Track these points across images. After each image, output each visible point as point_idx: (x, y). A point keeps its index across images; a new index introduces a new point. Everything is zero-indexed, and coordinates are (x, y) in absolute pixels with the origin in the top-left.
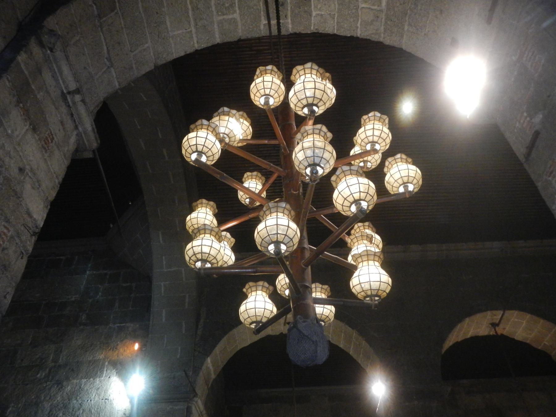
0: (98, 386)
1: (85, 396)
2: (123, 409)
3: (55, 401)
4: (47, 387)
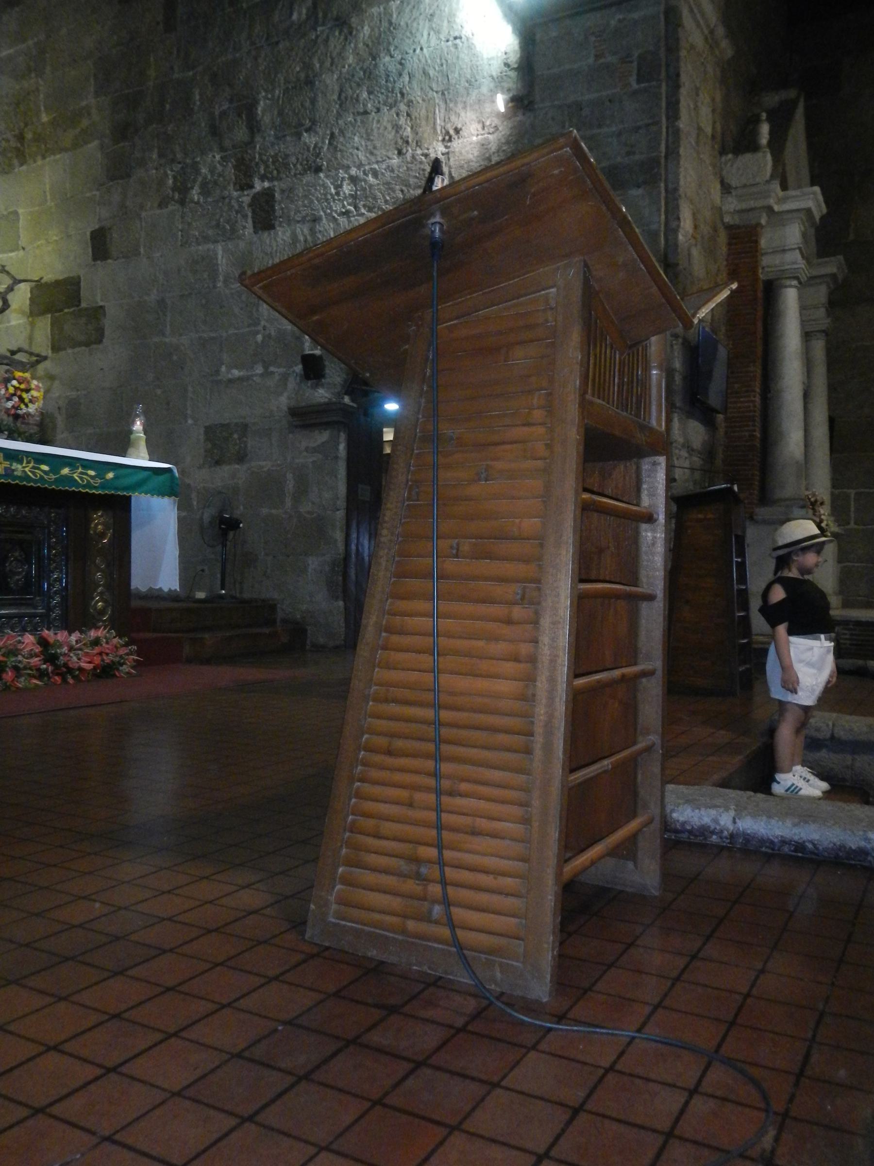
0: (430, 8)
1: (407, 41)
2: (500, 54)
3: (344, 67)
4: (319, 41)
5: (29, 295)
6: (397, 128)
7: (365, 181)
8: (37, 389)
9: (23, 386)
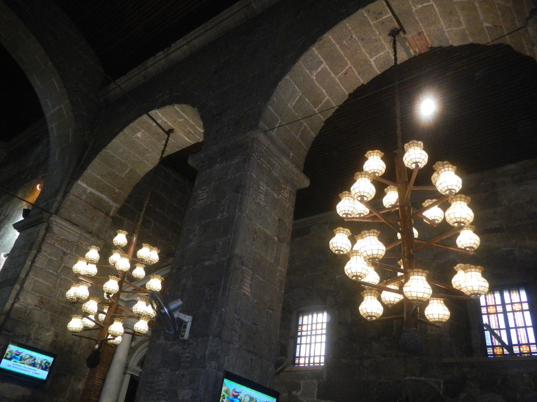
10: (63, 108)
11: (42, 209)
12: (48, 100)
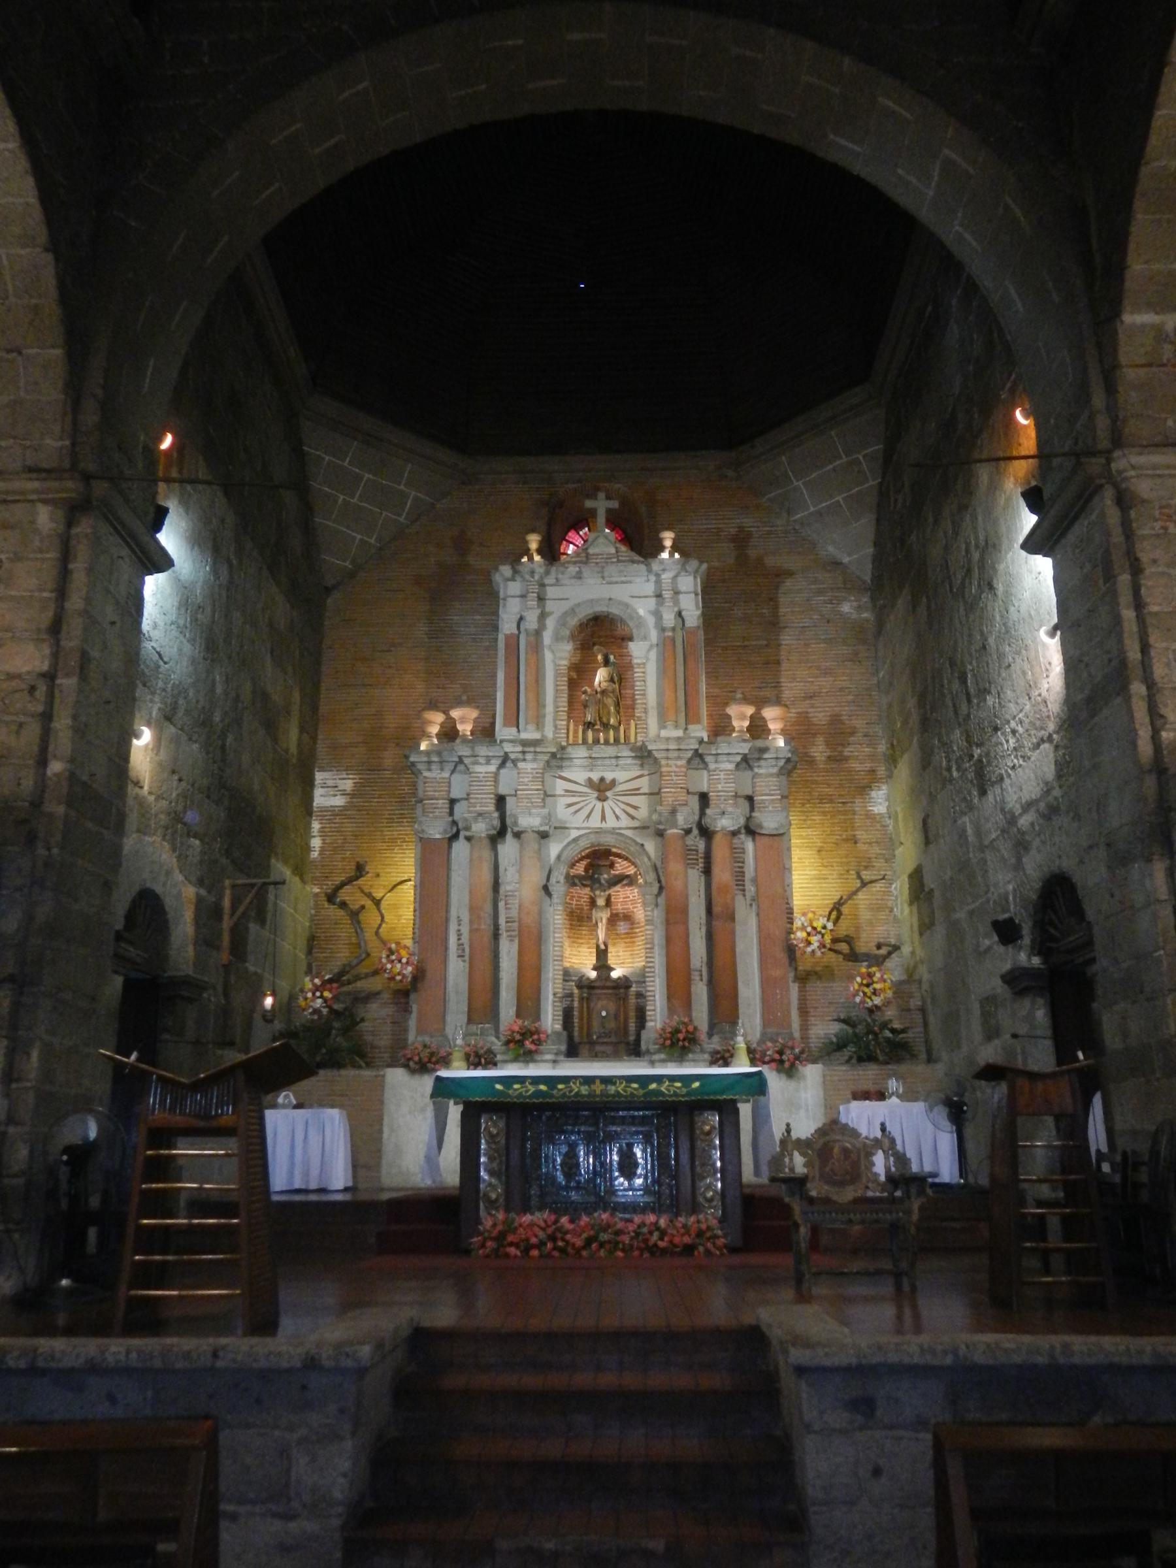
5: (907, 886)
6: (1024, 673)
7: (1017, 731)
8: (883, 980)
9: (865, 982)
10: (954, 156)
11: (1077, 455)
12: (900, 171)
